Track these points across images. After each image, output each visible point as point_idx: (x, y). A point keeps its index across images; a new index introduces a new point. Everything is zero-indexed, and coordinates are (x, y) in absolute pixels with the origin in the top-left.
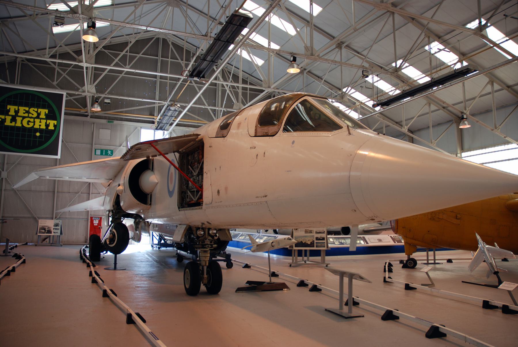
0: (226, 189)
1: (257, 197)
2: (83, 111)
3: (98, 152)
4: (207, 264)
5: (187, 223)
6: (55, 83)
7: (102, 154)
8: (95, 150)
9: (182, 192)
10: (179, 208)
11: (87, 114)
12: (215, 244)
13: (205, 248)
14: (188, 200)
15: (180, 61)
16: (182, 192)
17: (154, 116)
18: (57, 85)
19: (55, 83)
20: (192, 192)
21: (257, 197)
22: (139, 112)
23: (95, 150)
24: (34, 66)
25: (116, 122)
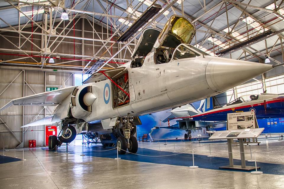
0: (144, 91)
1: (162, 91)
2: (38, 64)
3: (49, 89)
4: (129, 138)
5: (119, 115)
6: (19, 47)
7: (51, 90)
8: (47, 88)
9: (114, 100)
10: (113, 108)
11: (41, 66)
12: (133, 127)
13: (128, 129)
14: (119, 103)
15: (97, 33)
16: (114, 100)
17: (81, 65)
18: (21, 48)
19: (19, 47)
20: (122, 99)
21: (162, 91)
22: (72, 64)
23: (47, 88)
24: (6, 37)
25: (59, 70)
